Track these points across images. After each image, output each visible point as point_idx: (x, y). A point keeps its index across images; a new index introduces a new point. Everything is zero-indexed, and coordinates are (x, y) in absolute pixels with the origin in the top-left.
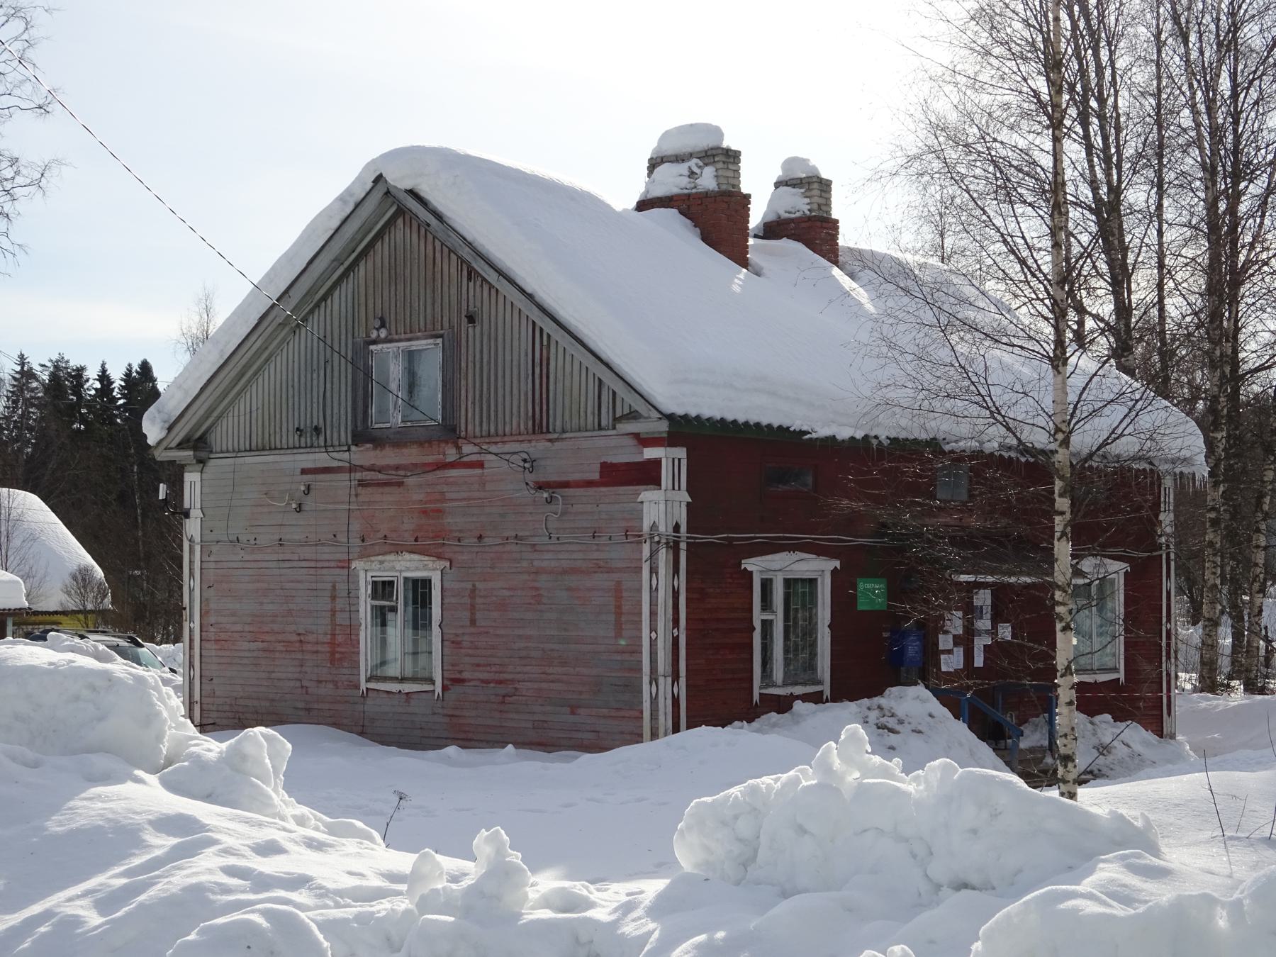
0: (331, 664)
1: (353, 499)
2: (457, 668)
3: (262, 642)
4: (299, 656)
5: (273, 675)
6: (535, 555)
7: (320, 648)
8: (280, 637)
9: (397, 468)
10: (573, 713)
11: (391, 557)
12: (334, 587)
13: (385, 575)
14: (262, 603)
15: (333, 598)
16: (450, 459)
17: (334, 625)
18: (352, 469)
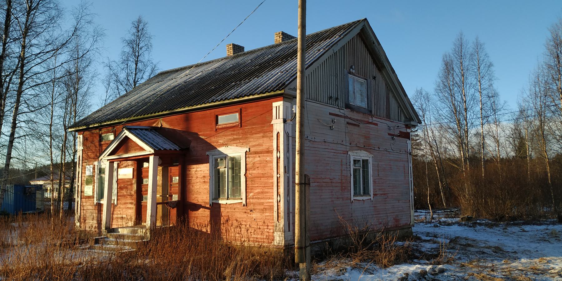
0: (342, 191)
1: (346, 128)
2: (375, 190)
3: (318, 183)
4: (331, 188)
5: (322, 197)
6: (390, 155)
7: (337, 185)
8: (324, 181)
9: (357, 120)
10: (399, 202)
11: (359, 151)
12: (342, 161)
13: (358, 158)
14: (317, 166)
15: (342, 165)
16: (370, 121)
17: (341, 176)
18: (346, 117)
